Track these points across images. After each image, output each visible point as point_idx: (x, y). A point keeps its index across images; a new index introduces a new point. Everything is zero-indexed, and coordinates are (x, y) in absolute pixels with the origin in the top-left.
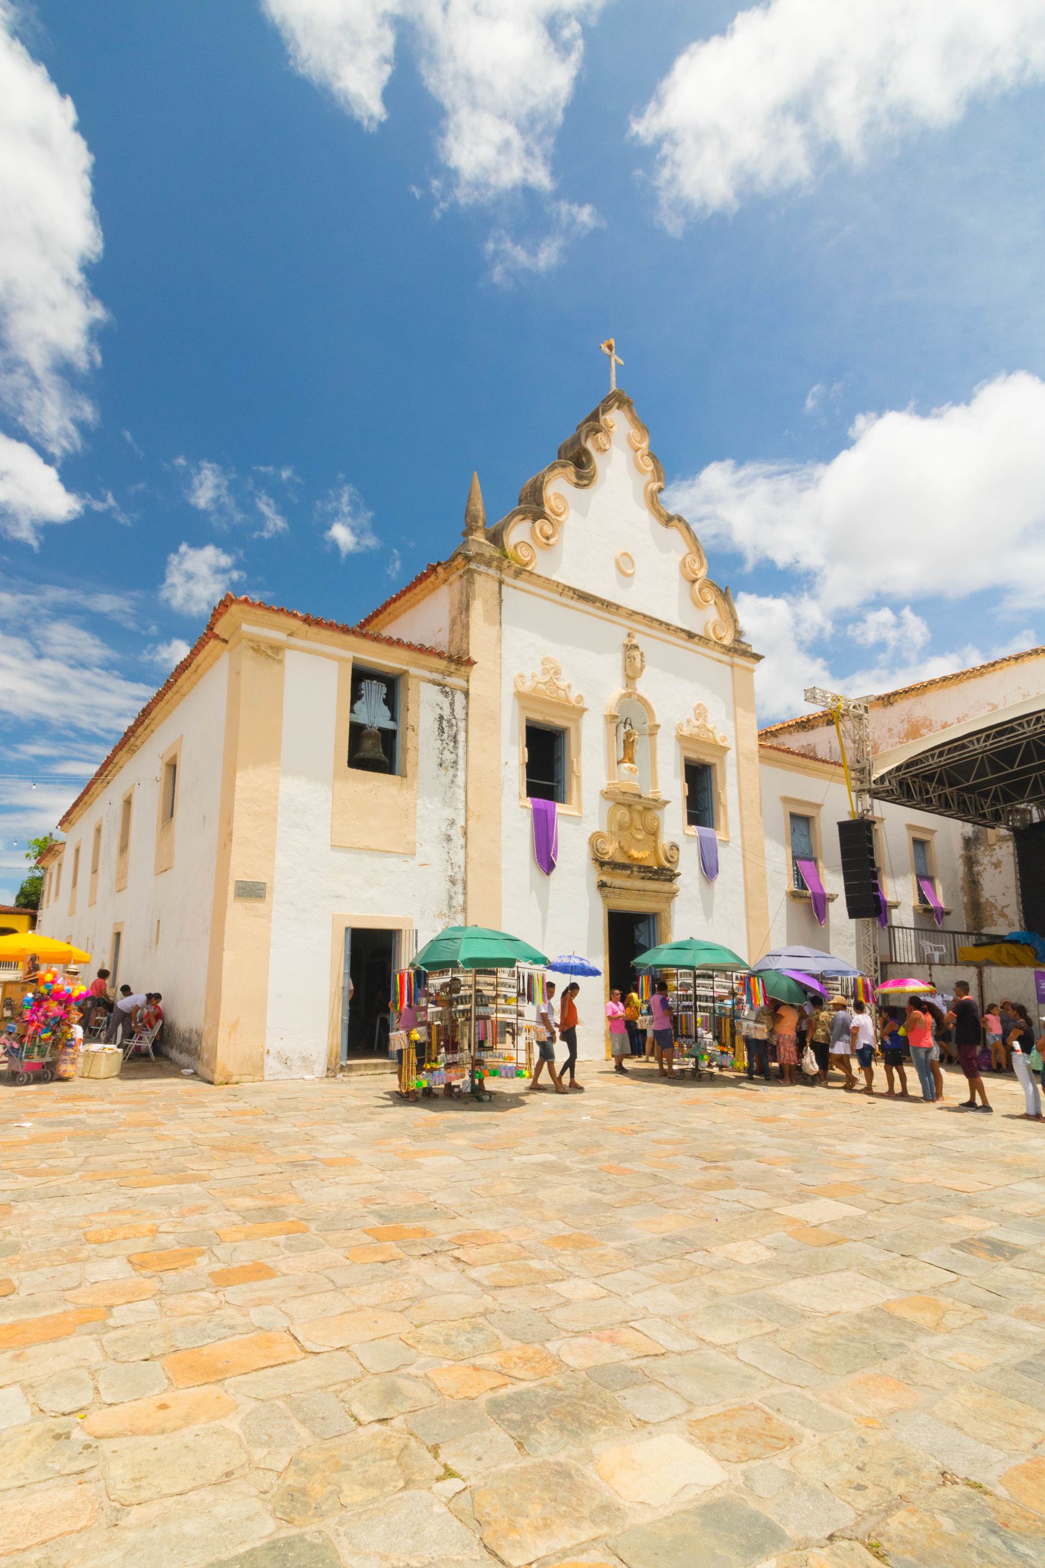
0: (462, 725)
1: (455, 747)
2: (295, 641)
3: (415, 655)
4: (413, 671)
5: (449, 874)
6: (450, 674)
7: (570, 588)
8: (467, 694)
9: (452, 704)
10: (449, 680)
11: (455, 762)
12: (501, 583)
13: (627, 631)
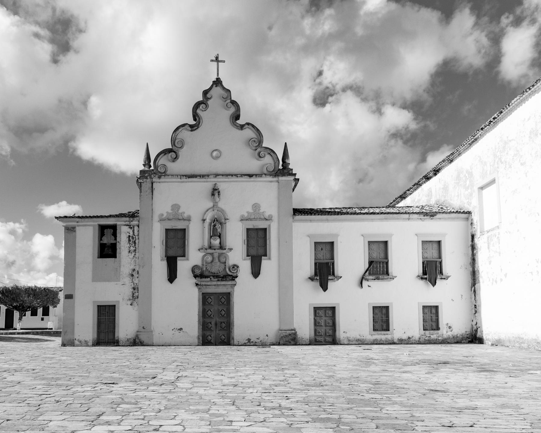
0: (137, 237)
1: (135, 245)
4: (118, 223)
6: (132, 221)
7: (183, 176)
8: (138, 226)
9: (133, 231)
10: (132, 223)
11: (135, 250)
12: (152, 184)
13: (206, 186)
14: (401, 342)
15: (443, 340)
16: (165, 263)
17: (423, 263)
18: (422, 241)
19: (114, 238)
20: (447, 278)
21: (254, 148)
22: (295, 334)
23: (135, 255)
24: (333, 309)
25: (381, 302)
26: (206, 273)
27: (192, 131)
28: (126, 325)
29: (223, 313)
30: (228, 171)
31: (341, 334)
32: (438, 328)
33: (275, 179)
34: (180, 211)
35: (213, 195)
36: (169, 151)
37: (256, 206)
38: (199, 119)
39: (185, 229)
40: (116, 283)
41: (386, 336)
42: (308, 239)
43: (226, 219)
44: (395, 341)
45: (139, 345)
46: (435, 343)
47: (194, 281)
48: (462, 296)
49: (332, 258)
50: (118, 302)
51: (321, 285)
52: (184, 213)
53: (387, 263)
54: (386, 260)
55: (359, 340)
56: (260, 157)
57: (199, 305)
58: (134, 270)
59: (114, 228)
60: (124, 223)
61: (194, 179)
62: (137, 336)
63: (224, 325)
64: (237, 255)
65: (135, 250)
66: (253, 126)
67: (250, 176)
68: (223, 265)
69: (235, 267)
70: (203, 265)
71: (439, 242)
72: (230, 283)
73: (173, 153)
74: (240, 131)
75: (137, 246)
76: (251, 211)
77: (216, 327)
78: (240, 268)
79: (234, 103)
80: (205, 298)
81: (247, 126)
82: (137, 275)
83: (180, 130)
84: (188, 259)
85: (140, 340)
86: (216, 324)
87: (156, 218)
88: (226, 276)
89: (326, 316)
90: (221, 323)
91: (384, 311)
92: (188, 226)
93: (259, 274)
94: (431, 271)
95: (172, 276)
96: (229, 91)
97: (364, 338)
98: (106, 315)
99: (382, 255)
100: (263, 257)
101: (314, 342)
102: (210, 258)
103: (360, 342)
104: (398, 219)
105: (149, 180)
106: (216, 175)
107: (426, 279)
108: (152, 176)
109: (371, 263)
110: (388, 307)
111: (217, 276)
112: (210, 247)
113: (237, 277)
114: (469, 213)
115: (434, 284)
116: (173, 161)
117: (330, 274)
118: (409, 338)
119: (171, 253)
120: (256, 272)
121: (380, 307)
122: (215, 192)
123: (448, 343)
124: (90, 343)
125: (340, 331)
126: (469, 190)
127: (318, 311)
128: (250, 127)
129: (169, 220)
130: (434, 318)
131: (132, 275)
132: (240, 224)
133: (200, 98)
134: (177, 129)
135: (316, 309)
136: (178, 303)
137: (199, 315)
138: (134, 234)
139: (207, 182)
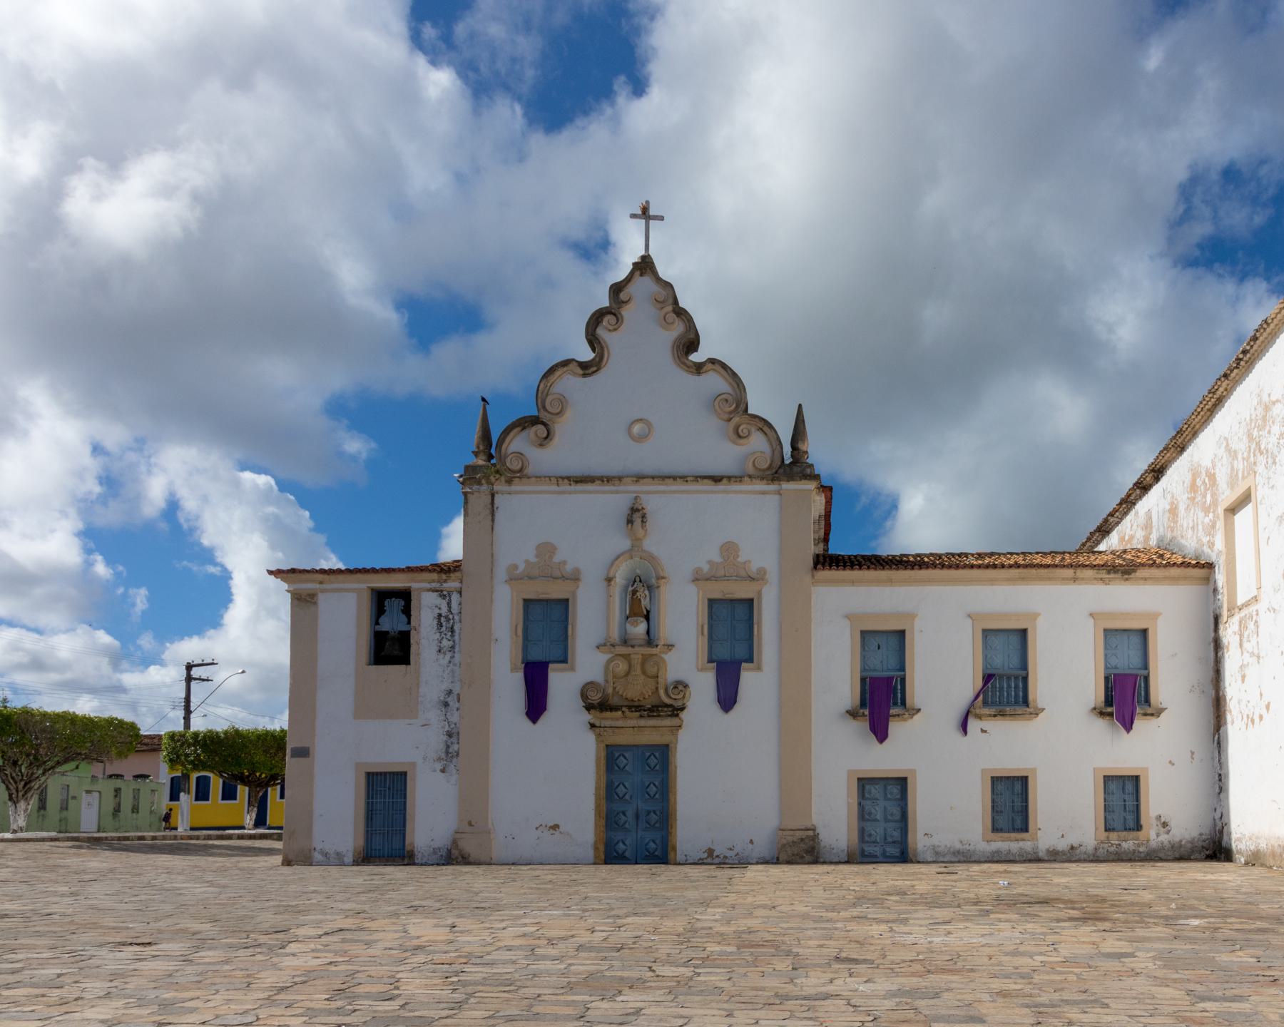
1: (452, 636)
2: (324, 586)
3: (411, 575)
4: (414, 585)
5: (447, 728)
6: (445, 581)
7: (563, 478)
9: (449, 604)
10: (445, 585)
11: (453, 647)
12: (493, 496)
13: (614, 502)
14: (1055, 856)
15: (1148, 854)
16: (520, 676)
17: (1107, 679)
18: (1105, 630)
19: (406, 620)
20: (1158, 713)
21: (726, 417)
22: (815, 838)
23: (453, 657)
24: (902, 782)
25: (1010, 764)
26: (615, 701)
27: (585, 375)
28: (430, 818)
29: (653, 789)
30: (666, 470)
31: (920, 840)
32: (1139, 827)
33: (773, 487)
34: (557, 559)
35: (630, 521)
36: (534, 421)
37: (729, 549)
38: (602, 348)
39: (567, 600)
40: (408, 721)
41: (1021, 844)
42: (848, 622)
43: (659, 578)
44: (1041, 854)
45: (458, 863)
46: (1130, 860)
47: (587, 717)
48: (1193, 753)
49: (903, 668)
50: (413, 765)
51: (874, 729)
52: (565, 562)
53: (1025, 679)
54: (1023, 673)
55: (958, 852)
56: (740, 437)
57: (598, 773)
58: (450, 692)
59: (405, 596)
60: (428, 586)
61: (589, 487)
62: (455, 842)
63: (654, 818)
64: (686, 660)
65: (453, 647)
66: (724, 366)
67: (717, 479)
68: (652, 682)
69: (681, 686)
70: (607, 681)
71: (1144, 632)
72: (668, 722)
73: (541, 427)
74: (696, 378)
75: (457, 637)
76: (718, 559)
77: (636, 824)
78: (692, 689)
79: (681, 313)
80: (612, 758)
81: (710, 366)
82: (457, 705)
83: (558, 373)
84: (572, 669)
85: (460, 851)
86: (637, 816)
87: (501, 574)
88: (657, 707)
89: (886, 799)
90: (649, 813)
91: (1018, 787)
92: (574, 593)
93: (735, 702)
94: (1125, 698)
95: (536, 706)
96: (668, 286)
97: (972, 848)
98: (386, 793)
99: (1015, 661)
100: (744, 665)
101: (860, 856)
102: (622, 667)
103: (965, 857)
104: (1050, 579)
105: (485, 487)
106: (639, 478)
107: (1111, 715)
108: (492, 479)
109: (988, 678)
110: (1026, 778)
111: (636, 707)
112: (625, 642)
113: (682, 709)
114: (1210, 566)
115: (1128, 726)
116: (541, 445)
117: (895, 704)
118: (1072, 848)
119: (537, 655)
120: (727, 699)
121: (1008, 778)
122: (635, 515)
123: (1161, 860)
124: (349, 859)
125: (915, 831)
126: (1211, 515)
127: (867, 787)
128: (717, 367)
129: (530, 578)
130: (1130, 803)
131: (446, 704)
132: (692, 589)
133: (605, 302)
134: (552, 370)
135: (865, 784)
136: (553, 767)
137: (597, 795)
138: (450, 611)
139: (617, 492)
